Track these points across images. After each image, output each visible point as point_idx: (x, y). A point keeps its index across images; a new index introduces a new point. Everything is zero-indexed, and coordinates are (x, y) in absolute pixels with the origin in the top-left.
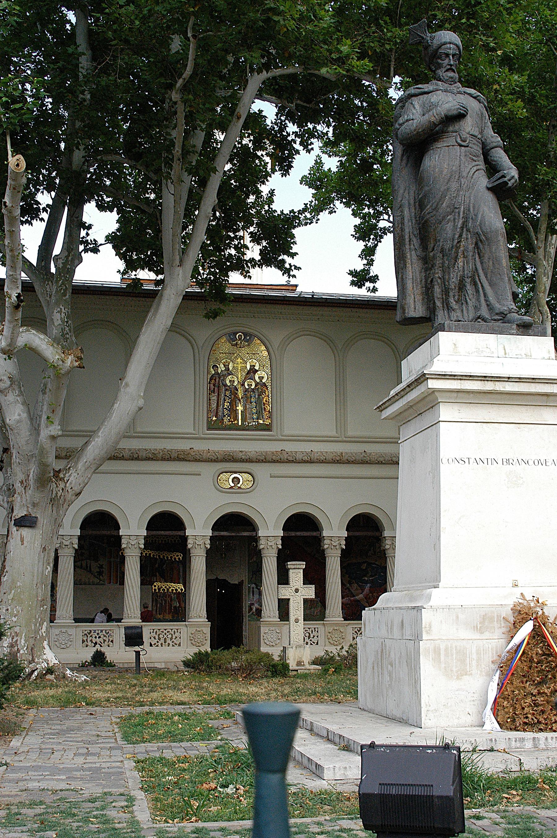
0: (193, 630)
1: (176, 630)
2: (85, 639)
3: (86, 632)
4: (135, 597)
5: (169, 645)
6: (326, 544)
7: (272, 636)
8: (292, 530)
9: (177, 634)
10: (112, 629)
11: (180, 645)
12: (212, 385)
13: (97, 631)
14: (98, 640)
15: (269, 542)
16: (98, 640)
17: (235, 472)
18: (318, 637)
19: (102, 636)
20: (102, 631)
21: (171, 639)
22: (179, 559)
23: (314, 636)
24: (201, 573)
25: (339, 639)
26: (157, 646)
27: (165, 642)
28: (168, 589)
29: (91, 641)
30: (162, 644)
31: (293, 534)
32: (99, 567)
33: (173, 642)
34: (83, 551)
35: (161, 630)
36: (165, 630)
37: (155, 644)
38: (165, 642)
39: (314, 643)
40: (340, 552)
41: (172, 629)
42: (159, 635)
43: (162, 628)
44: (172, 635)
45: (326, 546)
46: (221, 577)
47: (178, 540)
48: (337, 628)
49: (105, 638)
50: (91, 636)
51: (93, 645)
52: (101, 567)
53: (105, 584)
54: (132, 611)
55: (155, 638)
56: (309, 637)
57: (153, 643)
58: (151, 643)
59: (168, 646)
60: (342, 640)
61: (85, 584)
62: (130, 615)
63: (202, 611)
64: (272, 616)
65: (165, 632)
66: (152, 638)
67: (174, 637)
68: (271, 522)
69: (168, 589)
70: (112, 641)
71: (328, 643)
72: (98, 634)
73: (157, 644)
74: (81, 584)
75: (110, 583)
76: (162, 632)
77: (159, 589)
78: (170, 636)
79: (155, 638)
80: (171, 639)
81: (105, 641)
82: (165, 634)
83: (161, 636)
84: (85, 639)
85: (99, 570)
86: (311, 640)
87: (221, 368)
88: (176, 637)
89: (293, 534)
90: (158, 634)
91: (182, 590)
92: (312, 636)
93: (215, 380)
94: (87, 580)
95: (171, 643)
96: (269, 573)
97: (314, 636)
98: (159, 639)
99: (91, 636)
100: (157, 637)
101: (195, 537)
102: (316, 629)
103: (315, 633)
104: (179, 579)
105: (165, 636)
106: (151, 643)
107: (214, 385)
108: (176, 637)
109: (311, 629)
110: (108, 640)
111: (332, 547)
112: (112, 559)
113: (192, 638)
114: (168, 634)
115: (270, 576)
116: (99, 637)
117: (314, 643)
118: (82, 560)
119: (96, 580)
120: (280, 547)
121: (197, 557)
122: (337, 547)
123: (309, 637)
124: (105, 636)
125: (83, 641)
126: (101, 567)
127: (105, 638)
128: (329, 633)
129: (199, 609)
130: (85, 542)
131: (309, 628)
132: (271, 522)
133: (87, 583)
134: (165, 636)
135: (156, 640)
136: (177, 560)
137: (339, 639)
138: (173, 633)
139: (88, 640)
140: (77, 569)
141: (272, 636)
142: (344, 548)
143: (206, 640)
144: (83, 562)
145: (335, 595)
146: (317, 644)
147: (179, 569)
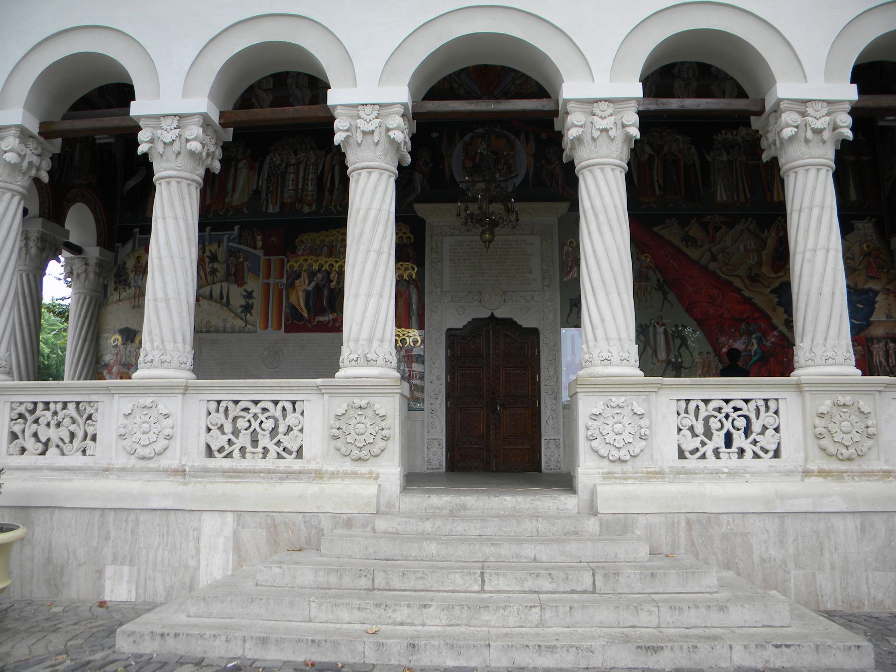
0: (341, 405)
1: (289, 406)
3: (22, 409)
4: (167, 300)
7: (618, 427)
8: (670, 94)
9: (291, 419)
10: (93, 398)
11: (299, 453)
13: (52, 406)
14: (53, 434)
15: (596, 119)
16: (53, 434)
18: (777, 430)
19: (67, 421)
21: (274, 432)
22: (410, 276)
23: (765, 428)
24: (376, 222)
25: (857, 438)
26: (229, 455)
27: (255, 442)
29: (35, 435)
30: (242, 450)
31: (674, 104)
32: (245, 297)
33: (278, 443)
34: (216, 265)
35: (242, 405)
36: (256, 402)
37: (221, 450)
38: (255, 442)
39: (766, 452)
40: (831, 155)
41: (276, 403)
42: (235, 419)
43: (246, 397)
44: (276, 420)
45: (787, 132)
46: (501, 313)
47: (409, 238)
48: (847, 399)
50: (36, 421)
51: (40, 447)
52: (249, 295)
53: (255, 332)
54: (156, 344)
55: (221, 428)
56: (747, 432)
57: (214, 447)
58: (208, 447)
59: (264, 457)
60: (870, 443)
61: (217, 331)
62: (150, 358)
63: (376, 344)
64: (616, 359)
65: (254, 409)
66: (215, 432)
67: (282, 429)
68: (601, 63)
70: (94, 438)
71: (817, 451)
73: (228, 449)
74: (208, 332)
75: (266, 328)
76: (246, 410)
78: (269, 425)
79: (221, 428)
80: (274, 432)
81: (72, 435)
82: (255, 416)
83: (242, 424)
85: (244, 303)
86: (755, 442)
88: (289, 429)
89: (674, 104)
90: (231, 415)
92: (756, 427)
94: (221, 324)
95: (273, 449)
96: (602, 218)
97: (765, 428)
98: (236, 432)
99: (36, 421)
100: (228, 428)
101: (354, 112)
102: (773, 405)
103: (767, 418)
104: (410, 318)
105: (255, 425)
106: (208, 447)
108: (289, 429)
109: (752, 405)
110: (80, 434)
111: (809, 134)
112: (271, 281)
113: (336, 432)
114: (262, 417)
115: (605, 228)
117: (766, 451)
118: (214, 283)
119: (239, 323)
120: (635, 133)
121: (364, 173)
122: (826, 135)
123: (747, 432)
124: (74, 421)
125: (14, 436)
126: (249, 295)
127: (73, 428)
128: (821, 415)
129: (365, 335)
130: (219, 246)
131: (747, 401)
132: (601, 63)
133: (221, 329)
134: (255, 425)
135: (226, 438)
136: (405, 277)
137: (857, 438)
138: (278, 413)
139: (28, 433)
140: (204, 303)
141: (618, 427)
142: (849, 135)
143: (385, 439)
144: (214, 287)
145: (827, 290)
146: (777, 454)
147: (410, 297)
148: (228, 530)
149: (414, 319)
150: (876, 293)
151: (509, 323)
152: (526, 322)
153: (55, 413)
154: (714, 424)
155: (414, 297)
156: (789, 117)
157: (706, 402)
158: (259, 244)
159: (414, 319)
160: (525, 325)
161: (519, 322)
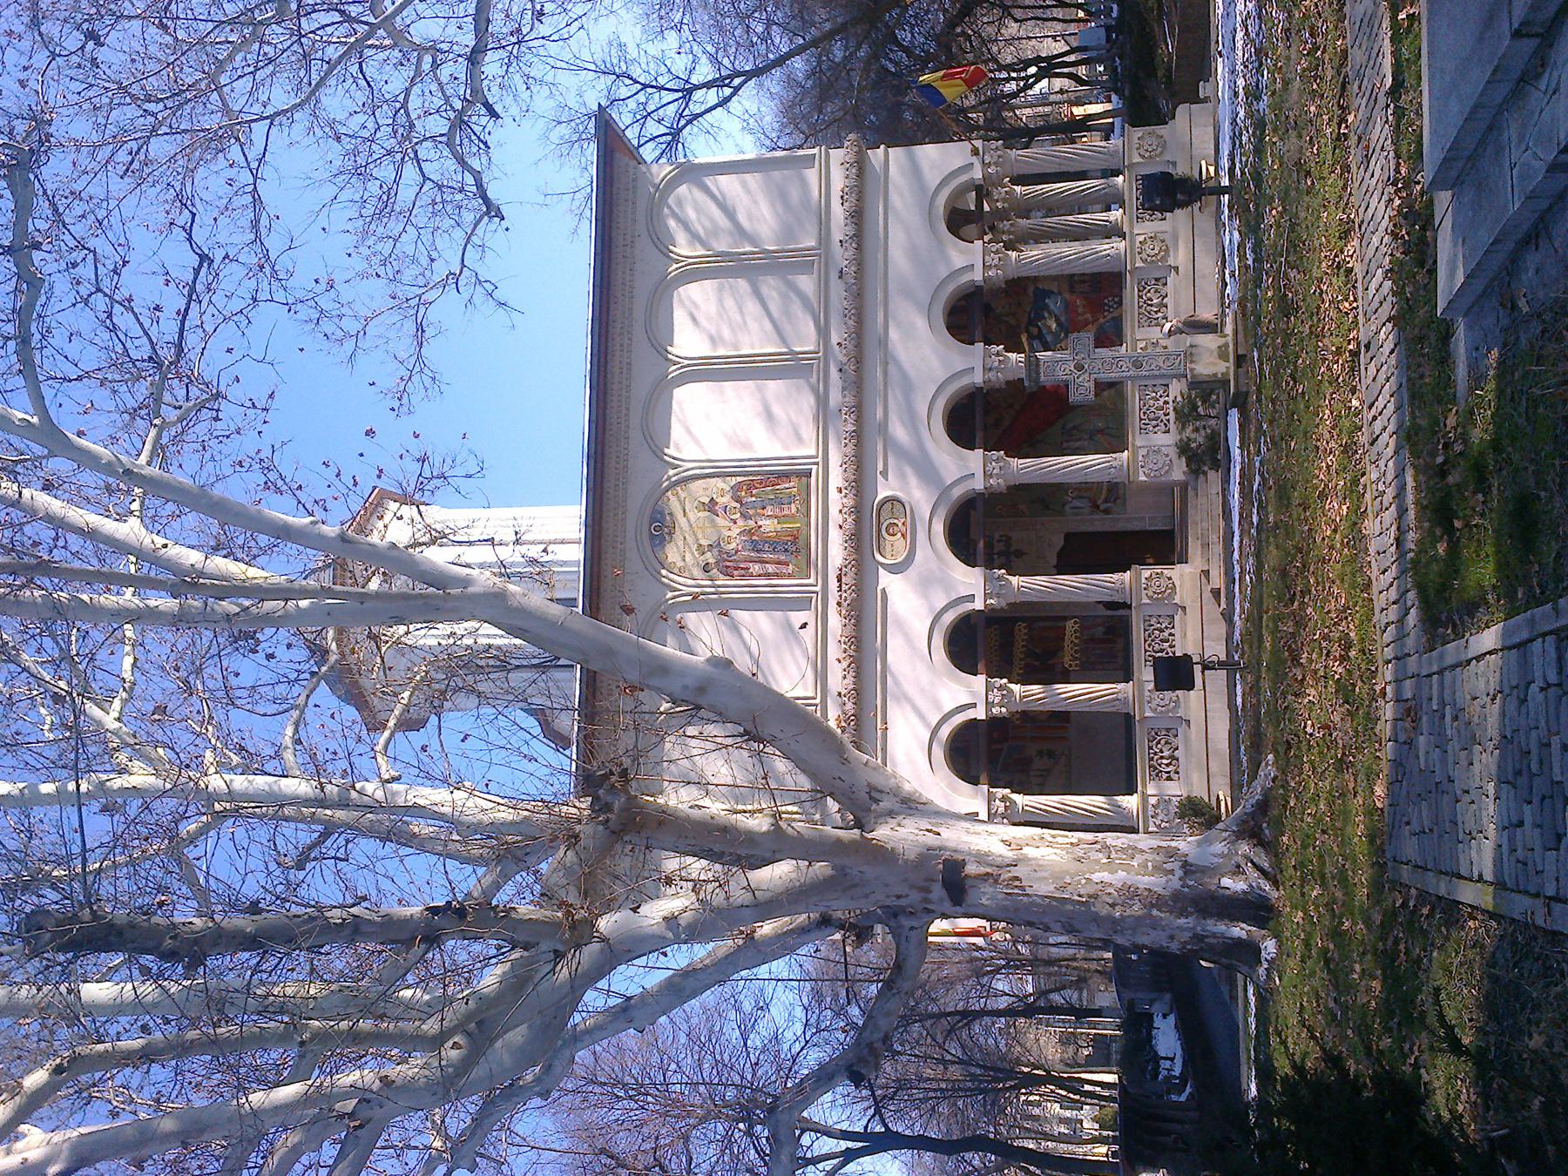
2: (1165, 776)
5: (1171, 634)
6: (998, 378)
12: (736, 573)
17: (879, 530)
20: (1150, 748)
28: (1076, 645)
41: (1145, 630)
49: (1163, 742)
52: (1040, 753)
69: (1076, 645)
70: (1168, 730)
72: (1155, 754)
77: (1076, 659)
84: (1165, 776)
87: (710, 558)
91: (1075, 623)
93: (728, 567)
107: (736, 569)
116: (1162, 752)
125: (1169, 779)
126: (1040, 753)
127: (1163, 742)
148: (1213, 644)
149: (1060, 624)
150: (1037, 288)
151: (1060, 555)
152: (1059, 542)
153: (1155, 754)
154: (1152, 415)
155: (1041, 624)
156: (992, 375)
157: (1141, 419)
158: (998, 746)
159: (1060, 624)
160: (1062, 543)
161: (1059, 547)
